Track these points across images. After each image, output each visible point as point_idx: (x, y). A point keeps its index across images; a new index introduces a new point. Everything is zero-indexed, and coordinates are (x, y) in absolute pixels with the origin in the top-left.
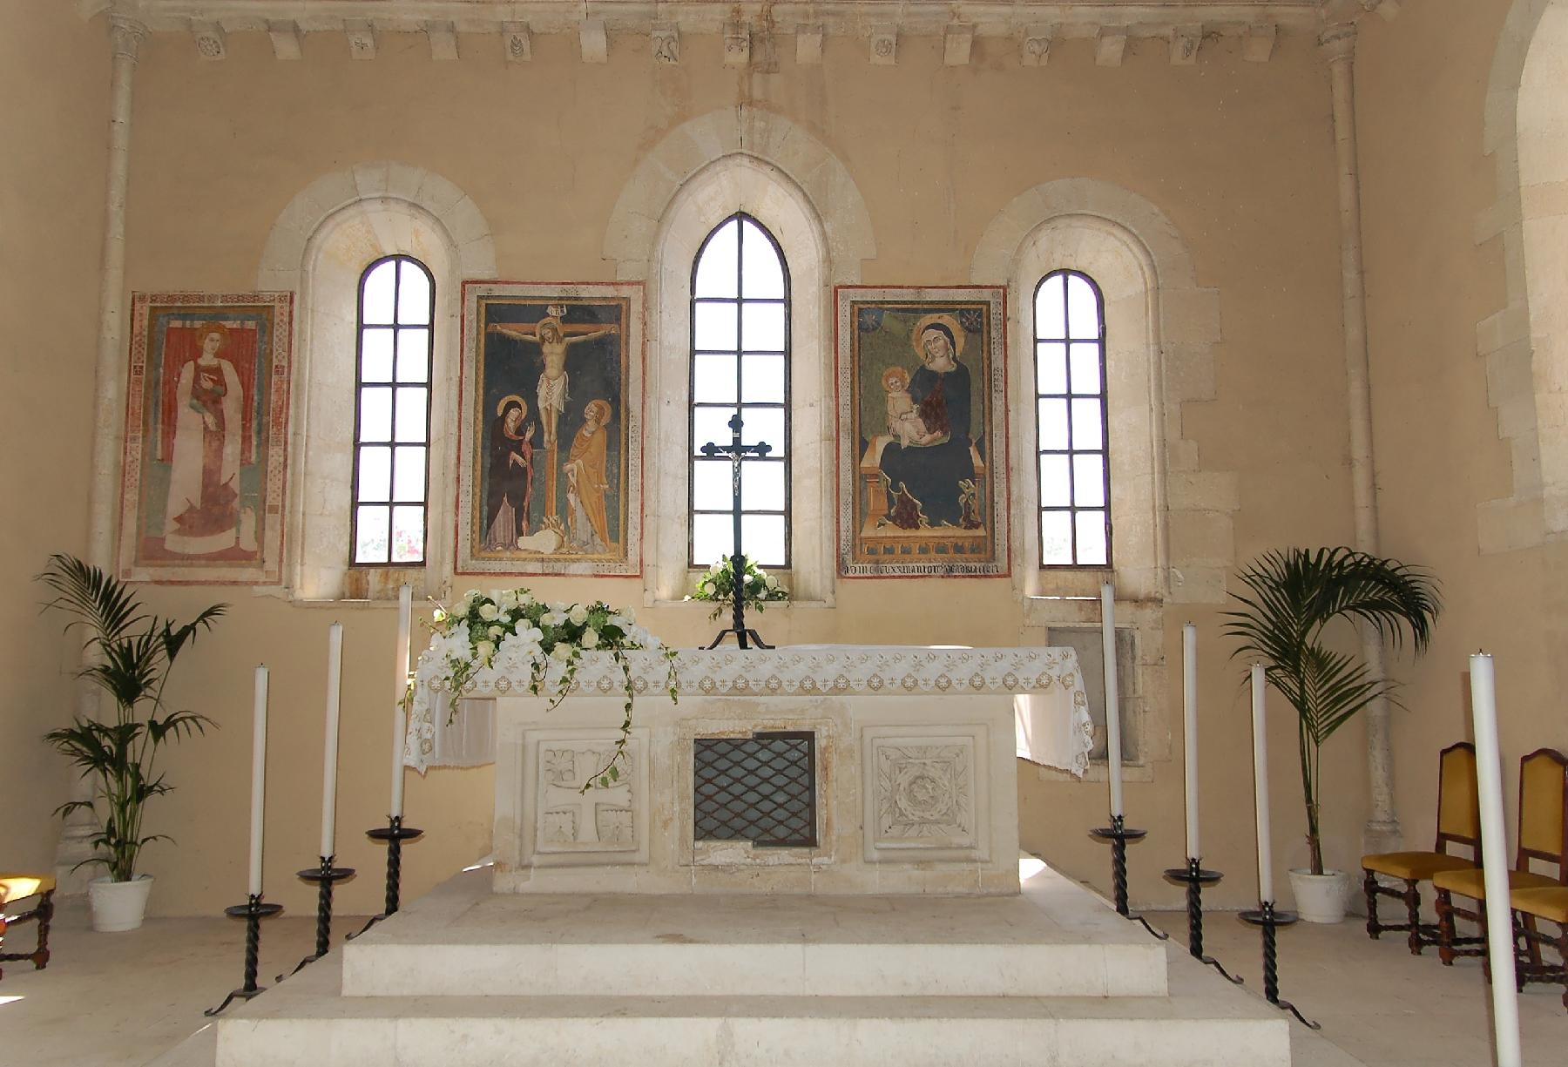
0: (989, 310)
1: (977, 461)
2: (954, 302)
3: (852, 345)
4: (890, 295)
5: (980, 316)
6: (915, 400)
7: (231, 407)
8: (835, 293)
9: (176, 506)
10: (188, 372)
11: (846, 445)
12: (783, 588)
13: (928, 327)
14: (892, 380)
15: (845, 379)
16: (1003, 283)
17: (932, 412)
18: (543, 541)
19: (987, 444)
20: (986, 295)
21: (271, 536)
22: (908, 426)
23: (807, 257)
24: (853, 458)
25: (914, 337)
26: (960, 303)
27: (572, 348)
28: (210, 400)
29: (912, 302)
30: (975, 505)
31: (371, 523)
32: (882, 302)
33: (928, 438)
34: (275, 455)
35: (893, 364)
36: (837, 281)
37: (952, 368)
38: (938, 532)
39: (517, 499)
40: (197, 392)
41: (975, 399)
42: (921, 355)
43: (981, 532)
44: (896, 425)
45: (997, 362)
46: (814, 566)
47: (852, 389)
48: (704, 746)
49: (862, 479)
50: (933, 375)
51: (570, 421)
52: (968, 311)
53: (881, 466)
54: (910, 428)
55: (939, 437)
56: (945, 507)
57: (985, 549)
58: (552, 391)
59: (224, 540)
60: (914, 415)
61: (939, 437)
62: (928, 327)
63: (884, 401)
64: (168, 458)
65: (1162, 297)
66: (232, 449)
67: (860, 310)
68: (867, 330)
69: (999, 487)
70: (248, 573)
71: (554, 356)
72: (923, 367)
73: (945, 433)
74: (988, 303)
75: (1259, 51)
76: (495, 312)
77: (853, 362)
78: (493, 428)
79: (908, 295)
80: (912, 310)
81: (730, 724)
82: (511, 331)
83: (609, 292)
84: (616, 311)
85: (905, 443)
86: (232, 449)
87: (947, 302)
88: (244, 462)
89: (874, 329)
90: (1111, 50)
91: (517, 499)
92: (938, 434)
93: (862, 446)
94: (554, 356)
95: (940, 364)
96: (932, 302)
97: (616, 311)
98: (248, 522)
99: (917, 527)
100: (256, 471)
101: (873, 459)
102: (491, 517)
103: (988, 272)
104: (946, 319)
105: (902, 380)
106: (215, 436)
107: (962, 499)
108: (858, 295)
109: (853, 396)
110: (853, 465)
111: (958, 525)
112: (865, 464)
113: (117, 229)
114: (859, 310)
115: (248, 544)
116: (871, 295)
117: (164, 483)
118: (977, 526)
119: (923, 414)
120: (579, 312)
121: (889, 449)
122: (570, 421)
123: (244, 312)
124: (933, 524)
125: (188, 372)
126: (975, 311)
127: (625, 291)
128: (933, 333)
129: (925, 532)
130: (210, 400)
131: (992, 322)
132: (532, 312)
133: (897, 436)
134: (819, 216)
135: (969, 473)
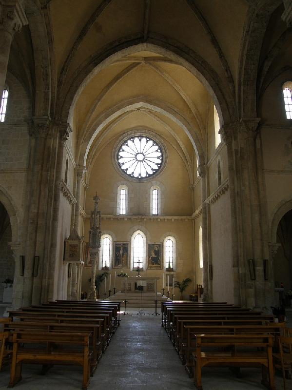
8: (147, 243)
18: (121, 265)
23: (145, 239)
31: (104, 263)
46: (145, 269)
54: (154, 256)
56: (157, 263)
57: (160, 267)
58: (121, 252)
71: (122, 248)
75: (186, 220)
76: (116, 244)
78: (116, 255)
82: (118, 246)
93: (149, 257)
94: (122, 248)
95: (157, 250)
97: (127, 244)
120: (124, 244)
122: (123, 254)
129: (155, 265)
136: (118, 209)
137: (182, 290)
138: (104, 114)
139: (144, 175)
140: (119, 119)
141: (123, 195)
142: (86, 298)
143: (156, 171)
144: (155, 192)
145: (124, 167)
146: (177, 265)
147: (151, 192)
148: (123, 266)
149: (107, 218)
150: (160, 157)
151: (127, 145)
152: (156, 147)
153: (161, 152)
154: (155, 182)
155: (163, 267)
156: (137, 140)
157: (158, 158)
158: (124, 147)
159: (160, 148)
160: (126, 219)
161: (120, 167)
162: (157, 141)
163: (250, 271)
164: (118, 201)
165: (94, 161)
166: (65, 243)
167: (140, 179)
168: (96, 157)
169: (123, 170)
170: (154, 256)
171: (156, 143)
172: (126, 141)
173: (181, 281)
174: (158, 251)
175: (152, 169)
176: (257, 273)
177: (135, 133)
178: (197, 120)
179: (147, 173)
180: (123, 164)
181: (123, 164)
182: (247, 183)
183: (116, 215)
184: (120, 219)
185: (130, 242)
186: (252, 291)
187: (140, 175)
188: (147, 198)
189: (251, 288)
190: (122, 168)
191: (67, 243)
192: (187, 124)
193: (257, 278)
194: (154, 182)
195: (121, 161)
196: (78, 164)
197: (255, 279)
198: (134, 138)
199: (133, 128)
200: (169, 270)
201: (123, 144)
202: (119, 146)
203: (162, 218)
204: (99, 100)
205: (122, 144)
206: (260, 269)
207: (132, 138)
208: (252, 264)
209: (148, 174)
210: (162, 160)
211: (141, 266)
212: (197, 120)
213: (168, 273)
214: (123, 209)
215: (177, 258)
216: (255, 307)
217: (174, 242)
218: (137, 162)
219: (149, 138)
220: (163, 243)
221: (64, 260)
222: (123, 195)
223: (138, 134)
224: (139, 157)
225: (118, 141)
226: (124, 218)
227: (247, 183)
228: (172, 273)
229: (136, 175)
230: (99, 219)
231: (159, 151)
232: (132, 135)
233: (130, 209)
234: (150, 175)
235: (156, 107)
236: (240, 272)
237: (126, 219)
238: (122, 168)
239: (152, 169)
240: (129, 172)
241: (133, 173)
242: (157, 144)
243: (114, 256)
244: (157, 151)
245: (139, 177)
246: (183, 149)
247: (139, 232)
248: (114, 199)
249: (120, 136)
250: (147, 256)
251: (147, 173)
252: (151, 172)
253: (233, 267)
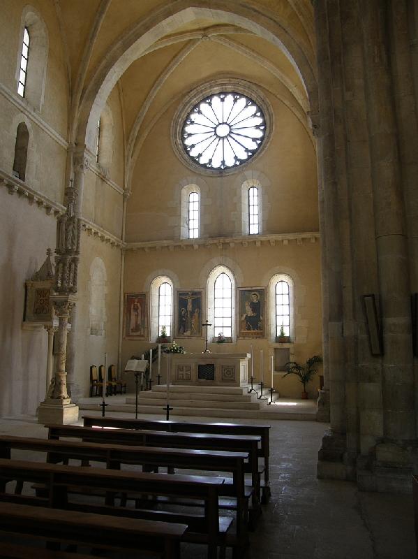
4: (246, 289)
7: (139, 311)
8: (237, 288)
9: (132, 327)
10: (132, 307)
12: (229, 340)
15: (238, 304)
17: (254, 310)
18: (188, 333)
21: (146, 332)
23: (233, 282)
27: (193, 300)
28: (136, 310)
34: (146, 318)
39: (184, 326)
40: (134, 309)
48: (199, 366)
49: (241, 322)
50: (254, 303)
51: (192, 313)
54: (250, 313)
55: (255, 314)
58: (190, 307)
59: (138, 333)
61: (255, 314)
64: (130, 319)
65: (295, 287)
66: (139, 318)
67: (241, 291)
69: (266, 323)
70: (142, 338)
71: (190, 301)
75: (313, 241)
76: (180, 294)
81: (203, 363)
83: (198, 290)
84: (200, 293)
86: (139, 318)
88: (142, 321)
90: (286, 242)
91: (184, 326)
93: (241, 316)
94: (190, 301)
95: (255, 301)
97: (200, 293)
98: (142, 329)
100: (143, 322)
101: (243, 318)
102: (180, 328)
103: (264, 285)
106: (137, 316)
113: (122, 283)
114: (241, 291)
115: (142, 334)
116: (244, 289)
117: (129, 323)
121: (247, 316)
122: (192, 313)
123: (141, 295)
125: (132, 307)
127: (202, 290)
130: (136, 310)
132: (186, 294)
134: (234, 275)
136: (183, 230)
137: (305, 379)
138: (120, 42)
139: (230, 162)
140: (176, 59)
141: (193, 203)
142: (150, 389)
143: (254, 152)
144: (254, 192)
145: (194, 153)
146: (296, 330)
147: (245, 194)
148: (193, 334)
149: (162, 247)
150: (260, 126)
151: (200, 112)
152: (253, 109)
153: (263, 116)
154: (250, 172)
155: (269, 334)
156: (216, 100)
157: (257, 127)
158: (194, 117)
159: (259, 110)
160: (196, 247)
161: (188, 153)
162: (254, 96)
163: (368, 333)
164: (184, 214)
165: (139, 146)
166: (26, 287)
167: (223, 171)
168: (142, 139)
169: (192, 158)
171: (252, 101)
172: (197, 106)
173: (303, 362)
174: (259, 302)
175: (247, 150)
176: (388, 336)
177: (211, 87)
178: (301, 17)
179: (236, 158)
180: (193, 146)
181: (193, 146)
182: (359, 82)
183: (179, 240)
184: (190, 245)
185: (205, 288)
186: (373, 389)
187: (223, 162)
188: (236, 204)
189: (370, 380)
190: (191, 154)
191: (29, 288)
192: (280, 30)
193: (388, 348)
194: (248, 173)
195: (188, 142)
196: (73, 140)
197: (382, 353)
198: (210, 97)
199: (207, 78)
200: (282, 339)
201: (192, 111)
202: (184, 116)
203: (263, 239)
204: (102, 13)
205: (189, 110)
206: (397, 323)
207: (207, 98)
208: (375, 309)
209: (239, 160)
210: (264, 131)
211: (227, 333)
212: (302, 19)
213: (278, 345)
214: (193, 230)
215: (296, 317)
216: (382, 441)
217: (291, 285)
218: (225, 140)
219: (236, 94)
220: (267, 287)
221: (24, 320)
222: (193, 203)
223: (217, 89)
224: (223, 130)
225: (180, 107)
226: (192, 246)
227: (359, 82)
228: (286, 345)
229: (216, 164)
230: (147, 244)
231: (259, 114)
232: (208, 92)
233: (204, 227)
234: (242, 162)
235: (219, 11)
236: (346, 333)
237: (196, 247)
238: (191, 154)
239: (247, 150)
240: (203, 161)
241: (211, 161)
242: (254, 103)
243: (176, 315)
244: (255, 115)
245: (222, 167)
246: (300, 102)
247: (221, 269)
248: (176, 211)
249: (184, 96)
250: (236, 315)
251: (236, 158)
252: (243, 156)
253: (330, 320)
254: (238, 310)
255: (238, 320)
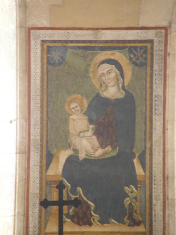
0: (152, 48)
1: (139, 171)
2: (124, 42)
3: (42, 77)
4: (74, 35)
5: (145, 52)
6: (91, 121)
11: (35, 158)
13: (103, 62)
14: (73, 105)
16: (165, 24)
17: (104, 131)
19: (148, 156)
20: (150, 35)
22: (85, 142)
24: (41, 168)
25: (91, 70)
26: (130, 41)
29: (90, 42)
30: (137, 206)
32: (66, 42)
33: (100, 151)
35: (75, 92)
36: (30, 24)
37: (121, 95)
38: (107, 228)
41: (139, 119)
42: (97, 85)
43: (141, 229)
44: (76, 141)
45: (158, 90)
47: (42, 112)
50: (106, 102)
52: (136, 48)
53: (63, 175)
54: (86, 143)
55: (109, 151)
60: (90, 133)
61: (109, 151)
62: (103, 62)
63: (66, 121)
68: (54, 65)
69: (157, 191)
72: (98, 96)
73: (114, 148)
74: (151, 42)
77: (42, 91)
79: (87, 36)
80: (89, 48)
85: (82, 156)
87: (118, 42)
89: (60, 63)
92: (109, 148)
93: (48, 158)
95: (112, 92)
96: (106, 42)
99: (90, 224)
101: (57, 169)
104: (118, 56)
105: (82, 106)
107: (127, 202)
108: (47, 35)
109: (42, 118)
110: (41, 173)
111: (123, 223)
112: (51, 172)
114: (48, 47)
116: (59, 35)
118: (138, 224)
119: (98, 133)
121: (70, 161)
124: (103, 221)
126: (141, 48)
128: (106, 67)
129: (96, 228)
131: (155, 57)
133: (75, 150)
135: (133, 180)
170: (86, 143)
254: (36, 132)
255: (35, 174)
